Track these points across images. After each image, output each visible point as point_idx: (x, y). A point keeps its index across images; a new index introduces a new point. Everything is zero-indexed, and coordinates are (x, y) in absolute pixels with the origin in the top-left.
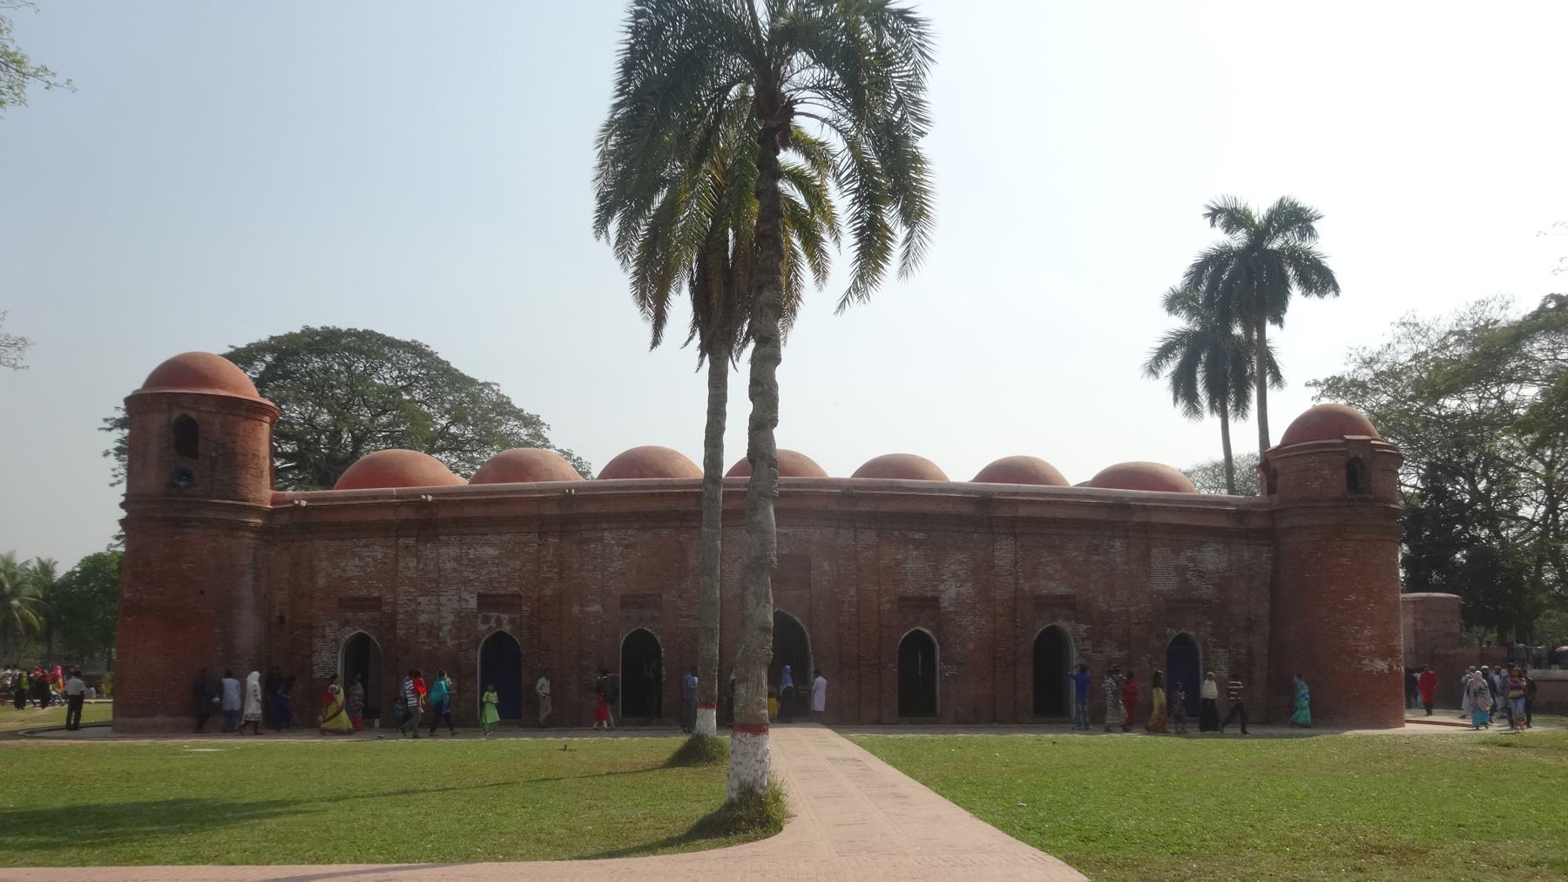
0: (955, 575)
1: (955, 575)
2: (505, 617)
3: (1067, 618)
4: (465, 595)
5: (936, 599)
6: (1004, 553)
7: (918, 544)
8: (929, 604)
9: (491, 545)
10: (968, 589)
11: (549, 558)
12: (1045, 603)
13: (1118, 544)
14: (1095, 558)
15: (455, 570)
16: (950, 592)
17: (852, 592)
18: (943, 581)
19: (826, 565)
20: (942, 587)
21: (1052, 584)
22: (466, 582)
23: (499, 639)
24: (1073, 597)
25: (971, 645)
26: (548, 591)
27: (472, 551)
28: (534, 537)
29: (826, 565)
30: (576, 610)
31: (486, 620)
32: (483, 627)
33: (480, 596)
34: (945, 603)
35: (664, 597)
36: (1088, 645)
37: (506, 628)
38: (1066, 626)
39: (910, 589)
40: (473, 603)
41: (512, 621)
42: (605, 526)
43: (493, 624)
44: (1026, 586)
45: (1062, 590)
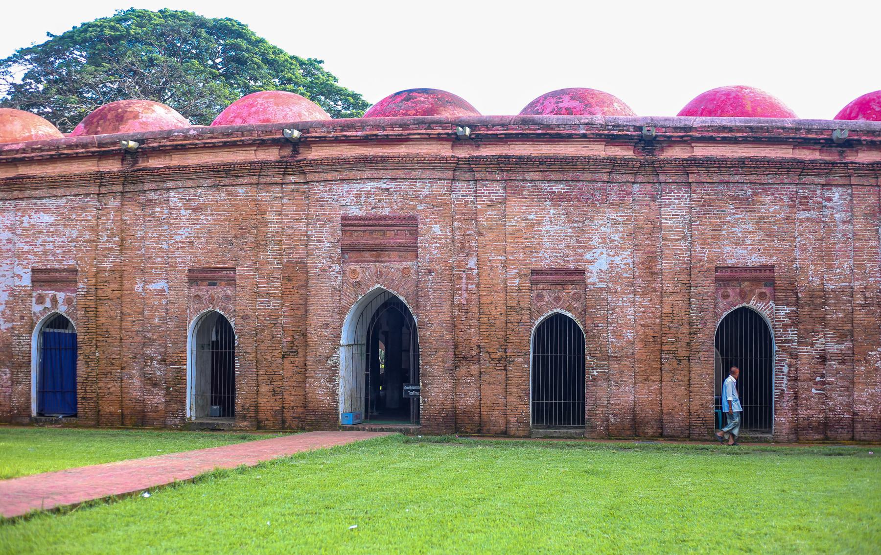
0: (606, 240)
1: (606, 240)
2: (61, 296)
3: (762, 296)
4: (19, 270)
5: (582, 272)
6: (675, 209)
7: (557, 199)
8: (571, 277)
9: (46, 210)
10: (624, 259)
11: (109, 225)
12: (729, 277)
13: (836, 195)
14: (803, 215)
15: (9, 241)
16: (599, 264)
17: (472, 262)
18: (590, 248)
19: (437, 229)
20: (588, 256)
21: (740, 251)
22: (20, 255)
23: (59, 321)
24: (771, 269)
25: (628, 334)
26: (108, 265)
27: (26, 219)
28: (92, 201)
29: (437, 229)
30: (139, 287)
31: (41, 300)
32: (37, 308)
33: (34, 271)
34: (592, 278)
35: (239, 271)
36: (791, 334)
37: (62, 309)
38: (764, 308)
39: (546, 259)
40: (26, 281)
41: (68, 301)
42: (170, 184)
43: (48, 304)
44: (705, 254)
45: (755, 260)
